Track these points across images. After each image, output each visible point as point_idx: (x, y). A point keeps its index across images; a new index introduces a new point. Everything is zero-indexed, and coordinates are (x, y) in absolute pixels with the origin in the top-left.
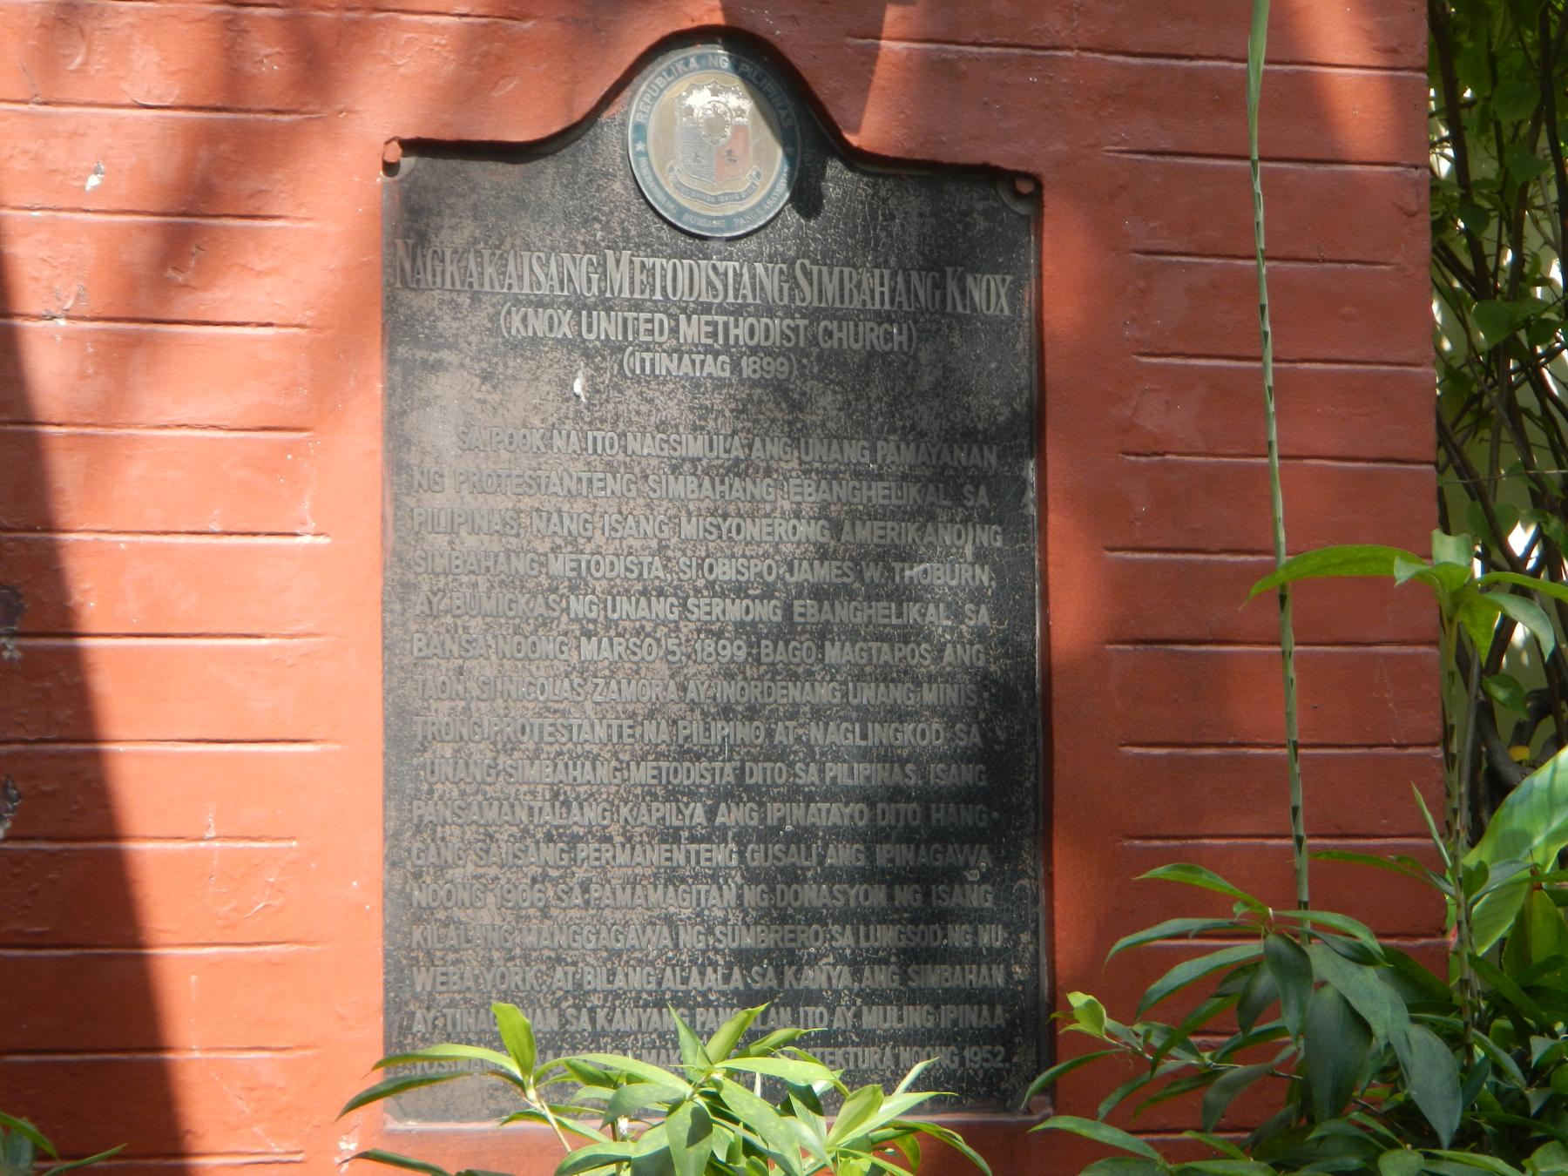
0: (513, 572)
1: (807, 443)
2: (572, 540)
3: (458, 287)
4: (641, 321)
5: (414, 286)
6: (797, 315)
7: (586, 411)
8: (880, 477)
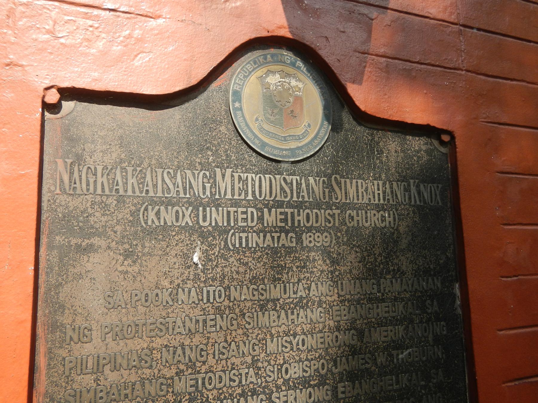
0: (147, 395)
1: (342, 284)
2: (191, 365)
3: (107, 192)
4: (239, 213)
5: (71, 192)
6: (334, 208)
7: (202, 274)
8: (383, 300)
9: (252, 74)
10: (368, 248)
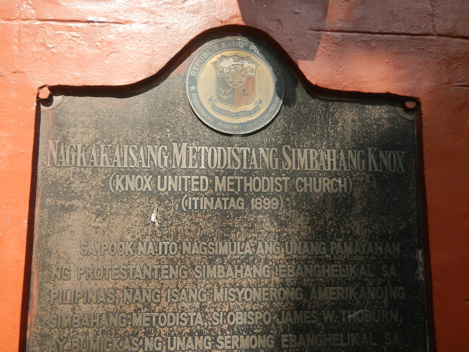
1: (289, 244)
2: (147, 305)
3: (85, 165)
4: (193, 180)
6: (283, 175)
8: (332, 262)
9: (208, 60)
10: (318, 212)
